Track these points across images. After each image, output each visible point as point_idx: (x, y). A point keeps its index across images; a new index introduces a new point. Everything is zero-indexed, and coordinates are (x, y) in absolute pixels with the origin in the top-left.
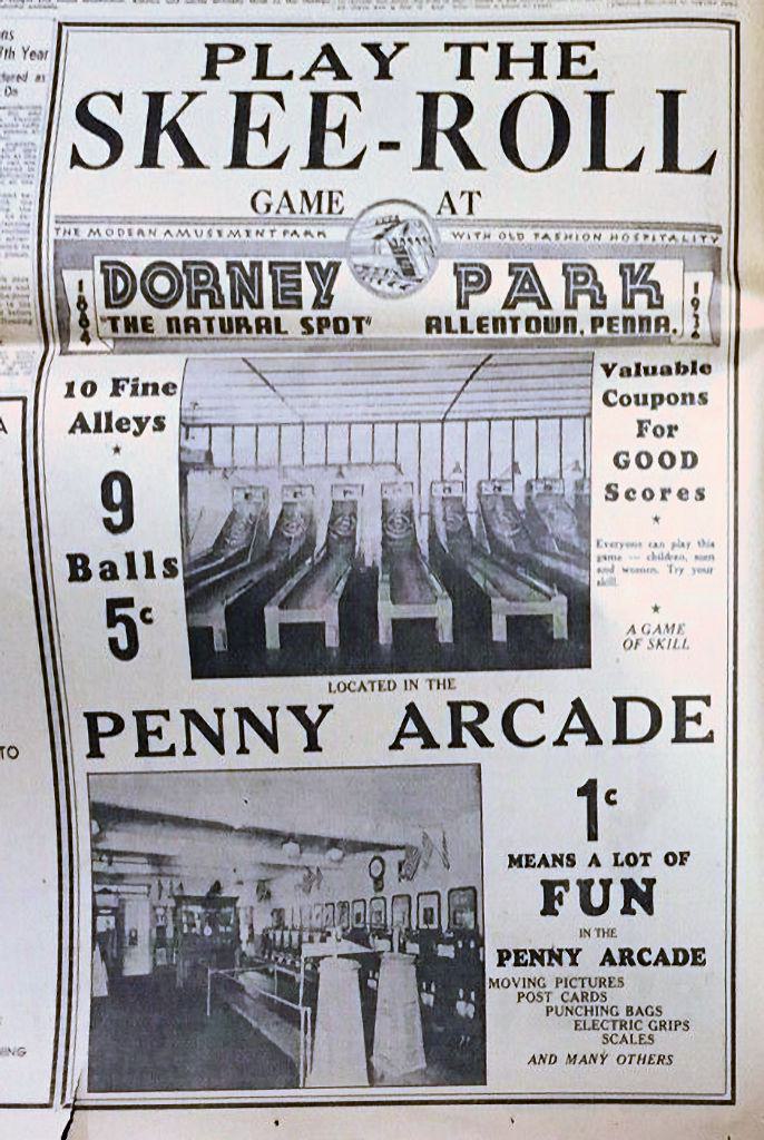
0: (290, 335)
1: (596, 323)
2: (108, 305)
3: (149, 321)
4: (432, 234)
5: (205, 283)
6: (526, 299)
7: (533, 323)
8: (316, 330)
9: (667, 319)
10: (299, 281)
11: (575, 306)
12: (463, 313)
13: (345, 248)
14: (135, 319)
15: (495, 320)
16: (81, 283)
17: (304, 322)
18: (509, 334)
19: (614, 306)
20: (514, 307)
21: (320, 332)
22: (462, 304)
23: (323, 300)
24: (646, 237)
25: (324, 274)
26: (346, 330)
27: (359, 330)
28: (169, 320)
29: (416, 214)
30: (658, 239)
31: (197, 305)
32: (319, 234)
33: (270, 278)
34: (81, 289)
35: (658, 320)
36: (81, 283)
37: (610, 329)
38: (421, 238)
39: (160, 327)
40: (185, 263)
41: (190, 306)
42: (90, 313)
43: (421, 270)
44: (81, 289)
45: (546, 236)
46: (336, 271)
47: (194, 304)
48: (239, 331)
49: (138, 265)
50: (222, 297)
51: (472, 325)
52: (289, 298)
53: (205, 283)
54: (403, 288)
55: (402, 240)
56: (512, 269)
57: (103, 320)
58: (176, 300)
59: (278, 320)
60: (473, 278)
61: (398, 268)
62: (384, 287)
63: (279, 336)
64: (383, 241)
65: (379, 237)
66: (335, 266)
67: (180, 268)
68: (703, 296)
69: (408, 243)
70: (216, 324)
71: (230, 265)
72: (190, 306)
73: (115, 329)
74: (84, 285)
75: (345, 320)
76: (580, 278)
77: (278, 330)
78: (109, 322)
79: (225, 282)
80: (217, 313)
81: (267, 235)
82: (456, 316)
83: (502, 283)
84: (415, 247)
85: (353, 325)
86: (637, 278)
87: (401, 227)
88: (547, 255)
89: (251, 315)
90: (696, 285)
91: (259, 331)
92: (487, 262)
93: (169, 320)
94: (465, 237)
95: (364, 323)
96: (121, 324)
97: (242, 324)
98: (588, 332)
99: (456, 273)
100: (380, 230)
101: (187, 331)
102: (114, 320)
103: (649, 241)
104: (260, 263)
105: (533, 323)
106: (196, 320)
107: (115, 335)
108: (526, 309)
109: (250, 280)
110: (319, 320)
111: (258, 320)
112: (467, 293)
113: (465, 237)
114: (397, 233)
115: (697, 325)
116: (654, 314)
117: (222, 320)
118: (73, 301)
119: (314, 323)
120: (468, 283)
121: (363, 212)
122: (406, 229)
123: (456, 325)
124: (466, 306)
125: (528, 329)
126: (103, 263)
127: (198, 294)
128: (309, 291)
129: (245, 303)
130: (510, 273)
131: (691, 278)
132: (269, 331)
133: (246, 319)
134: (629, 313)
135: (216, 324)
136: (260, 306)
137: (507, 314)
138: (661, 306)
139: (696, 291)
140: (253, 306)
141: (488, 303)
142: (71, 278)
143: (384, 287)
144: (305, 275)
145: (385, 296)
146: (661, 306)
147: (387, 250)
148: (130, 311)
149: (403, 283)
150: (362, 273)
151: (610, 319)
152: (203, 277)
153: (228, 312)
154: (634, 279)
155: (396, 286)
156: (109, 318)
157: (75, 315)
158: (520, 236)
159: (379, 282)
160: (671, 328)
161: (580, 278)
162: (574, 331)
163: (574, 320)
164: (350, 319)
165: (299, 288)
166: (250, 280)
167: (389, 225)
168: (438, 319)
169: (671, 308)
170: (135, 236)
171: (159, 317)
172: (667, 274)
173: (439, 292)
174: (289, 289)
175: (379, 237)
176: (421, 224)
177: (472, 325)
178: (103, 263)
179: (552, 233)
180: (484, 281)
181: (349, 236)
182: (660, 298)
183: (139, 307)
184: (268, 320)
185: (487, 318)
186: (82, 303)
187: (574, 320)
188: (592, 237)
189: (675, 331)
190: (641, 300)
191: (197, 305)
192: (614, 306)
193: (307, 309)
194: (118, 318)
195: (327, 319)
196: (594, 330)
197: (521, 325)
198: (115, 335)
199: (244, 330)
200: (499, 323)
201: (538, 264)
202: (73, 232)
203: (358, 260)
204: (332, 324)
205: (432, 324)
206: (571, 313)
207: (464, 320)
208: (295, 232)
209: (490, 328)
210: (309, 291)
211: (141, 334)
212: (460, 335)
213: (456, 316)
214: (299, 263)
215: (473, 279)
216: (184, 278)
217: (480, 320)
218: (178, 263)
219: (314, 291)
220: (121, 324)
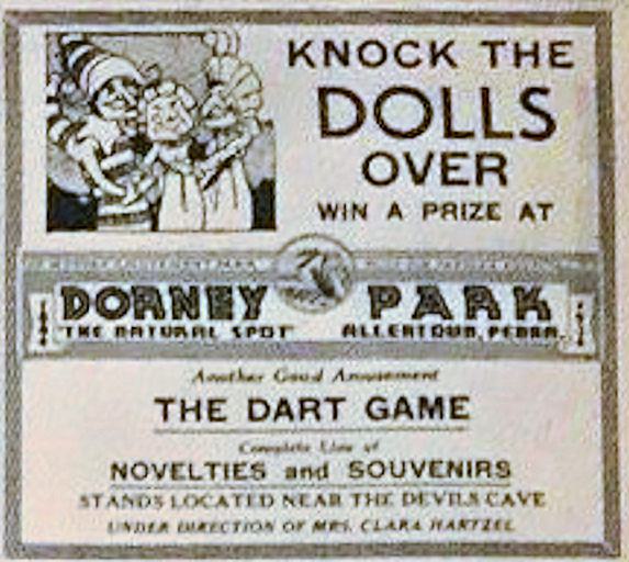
1: (493, 331)
10: (230, 303)
12: (377, 322)
17: (235, 330)
18: (416, 337)
19: (508, 318)
21: (249, 335)
22: (375, 315)
23: (253, 313)
25: (253, 294)
26: (272, 335)
27: (283, 335)
29: (338, 249)
31: (143, 317)
40: (134, 289)
42: (50, 325)
43: (340, 290)
47: (139, 316)
49: (92, 289)
51: (384, 329)
54: (323, 304)
56: (419, 290)
57: (61, 328)
58: (125, 313)
59: (212, 330)
61: (319, 292)
62: (306, 303)
64: (306, 271)
65: (303, 265)
66: (263, 289)
70: (157, 332)
71: (171, 290)
78: (65, 331)
79: (167, 301)
80: (158, 324)
81: (203, 266)
83: (410, 299)
86: (528, 300)
88: (452, 278)
89: (188, 324)
95: (288, 334)
96: (75, 333)
97: (180, 331)
98: (486, 338)
100: (302, 260)
108: (430, 320)
114: (316, 262)
115: (582, 333)
116: (544, 325)
117: (163, 329)
118: (36, 311)
122: (325, 260)
123: (370, 330)
124: (379, 316)
125: (434, 334)
127: (144, 309)
128: (240, 307)
129: (184, 315)
131: (575, 299)
135: (157, 332)
136: (197, 316)
137: (415, 323)
141: (400, 315)
142: (35, 299)
144: (237, 296)
146: (549, 317)
148: (83, 322)
153: (169, 321)
154: (526, 298)
157: (37, 324)
161: (477, 298)
169: (558, 320)
171: (109, 327)
172: (553, 294)
173: (355, 307)
175: (303, 265)
177: (384, 329)
180: (395, 299)
183: (92, 318)
186: (43, 317)
190: (532, 316)
191: (143, 317)
192: (508, 318)
193: (238, 319)
197: (428, 332)
200: (407, 330)
203: (287, 284)
205: (348, 330)
207: (376, 329)
210: (240, 307)
215: (383, 298)
217: (391, 330)
218: (126, 288)
220: (75, 333)
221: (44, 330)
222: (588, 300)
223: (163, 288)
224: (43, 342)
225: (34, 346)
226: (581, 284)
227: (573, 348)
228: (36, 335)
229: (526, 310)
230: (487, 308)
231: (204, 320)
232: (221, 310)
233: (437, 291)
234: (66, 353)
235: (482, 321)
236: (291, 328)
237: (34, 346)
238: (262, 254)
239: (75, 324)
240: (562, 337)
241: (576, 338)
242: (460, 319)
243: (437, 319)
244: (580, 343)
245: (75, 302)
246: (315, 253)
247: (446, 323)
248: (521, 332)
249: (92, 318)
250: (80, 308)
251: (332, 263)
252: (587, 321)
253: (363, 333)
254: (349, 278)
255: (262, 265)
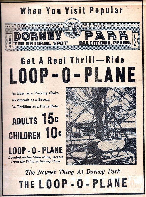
0: (51, 45)
1: (114, 42)
2: (15, 40)
3: (23, 43)
4: (81, 26)
5: (34, 36)
6: (99, 38)
7: (101, 42)
8: (57, 44)
9: (129, 42)
10: (53, 35)
11: (110, 39)
12: (87, 41)
13: (63, 29)
14: (20, 42)
15: (94, 42)
16: (10, 36)
17: (54, 43)
18: (96, 44)
19: (118, 39)
20: (97, 39)
21: (57, 44)
23: (58, 38)
24: (124, 25)
25: (59, 34)
26: (63, 44)
27: (65, 44)
28: (27, 43)
30: (127, 26)
32: (57, 26)
33: (48, 34)
34: (10, 37)
35: (127, 42)
36: (10, 36)
37: (117, 44)
38: (78, 26)
39: (25, 44)
41: (31, 40)
42: (11, 42)
43: (79, 33)
44: (10, 37)
45: (104, 26)
46: (61, 34)
48: (41, 44)
49: (21, 33)
50: (38, 38)
51: (89, 43)
52: (52, 38)
53: (34, 36)
55: (74, 27)
57: (14, 43)
59: (49, 42)
60: (89, 34)
63: (49, 45)
64: (71, 27)
67: (29, 33)
68: (137, 37)
69: (76, 28)
70: (36, 43)
72: (31, 40)
73: (16, 44)
74: (11, 36)
75: (63, 42)
76: (111, 34)
77: (49, 44)
79: (38, 35)
80: (37, 41)
81: (47, 26)
82: (85, 41)
83: (95, 35)
84: (77, 28)
85: (64, 43)
87: (74, 24)
90: (135, 35)
91: (45, 44)
92: (92, 31)
93: (27, 43)
94: (87, 26)
95: (66, 43)
96: (17, 44)
98: (113, 44)
99: (85, 33)
100: (70, 25)
101: (30, 45)
102: (16, 43)
103: (125, 26)
104: (45, 32)
105: (101, 42)
106: (32, 43)
107: (16, 46)
108: (100, 40)
109: (44, 35)
110: (57, 42)
111: (45, 42)
112: (88, 37)
113: (87, 26)
114: (73, 25)
115: (135, 43)
116: (126, 41)
117: (37, 42)
118: (8, 39)
119: (56, 43)
120: (89, 35)
121: (67, 20)
122: (75, 25)
123: (85, 43)
124: (88, 40)
125: (100, 44)
126: (14, 32)
127: (33, 38)
128: (55, 37)
130: (97, 33)
131: (134, 34)
132: (47, 44)
133: (42, 42)
134: (121, 40)
135: (36, 43)
136: (46, 40)
137: (96, 41)
138: (128, 39)
139: (135, 36)
140: (44, 40)
141: (92, 39)
142: (8, 35)
143: (71, 36)
144: (55, 34)
145: (71, 38)
146: (128, 39)
147: (71, 29)
149: (75, 35)
150: (67, 33)
151: (117, 42)
152: (34, 35)
153: (39, 41)
155: (73, 36)
156: (15, 42)
157: (9, 42)
158: (98, 26)
159: (70, 35)
160: (130, 43)
161: (111, 34)
162: (110, 44)
163: (110, 42)
164: (64, 42)
165: (53, 36)
166: (44, 35)
167: (71, 24)
168: (82, 42)
169: (130, 39)
170: (21, 27)
171: (25, 42)
173: (82, 37)
174: (52, 37)
175: (70, 26)
176: (78, 24)
177: (89, 43)
178: (14, 32)
179: (105, 25)
181: (63, 27)
182: (127, 37)
183: (21, 40)
184: (47, 42)
185: (92, 42)
186: (10, 40)
187: (110, 42)
188: (113, 26)
189: (131, 44)
190: (123, 38)
192: (118, 39)
194: (17, 42)
195: (59, 42)
196: (114, 44)
197: (99, 43)
198: (16, 46)
199: (42, 44)
200: (94, 43)
201: (102, 31)
202: (8, 26)
203: (66, 31)
204: (60, 43)
205: (81, 43)
206: (109, 41)
207: (87, 42)
208: (53, 26)
209: (92, 43)
210: (55, 37)
211: (21, 45)
212: (86, 45)
213: (85, 41)
214: (53, 32)
215: (89, 34)
216: (30, 35)
217: (91, 42)
218: (29, 32)
219: (56, 37)
220: (17, 44)
221: (10, 43)
222: (137, 34)
223: (38, 32)
224: (10, 46)
225: (8, 48)
226: (136, 30)
227: (133, 47)
228: (8, 45)
229: (122, 37)
230: (113, 37)
231: (47, 41)
232: (51, 38)
233: (101, 32)
234: (15, 49)
235: (112, 40)
236: (68, 42)
237: (8, 48)
238: (60, 23)
239: (17, 41)
240: (131, 44)
241: (134, 44)
242: (107, 40)
243: (101, 40)
244: (135, 45)
245: (18, 36)
246: (72, 23)
247: (103, 41)
248: (121, 43)
249: (21, 40)
250: (19, 36)
251: (77, 25)
252: (136, 40)
253: (84, 44)
254: (81, 30)
255: (61, 26)
